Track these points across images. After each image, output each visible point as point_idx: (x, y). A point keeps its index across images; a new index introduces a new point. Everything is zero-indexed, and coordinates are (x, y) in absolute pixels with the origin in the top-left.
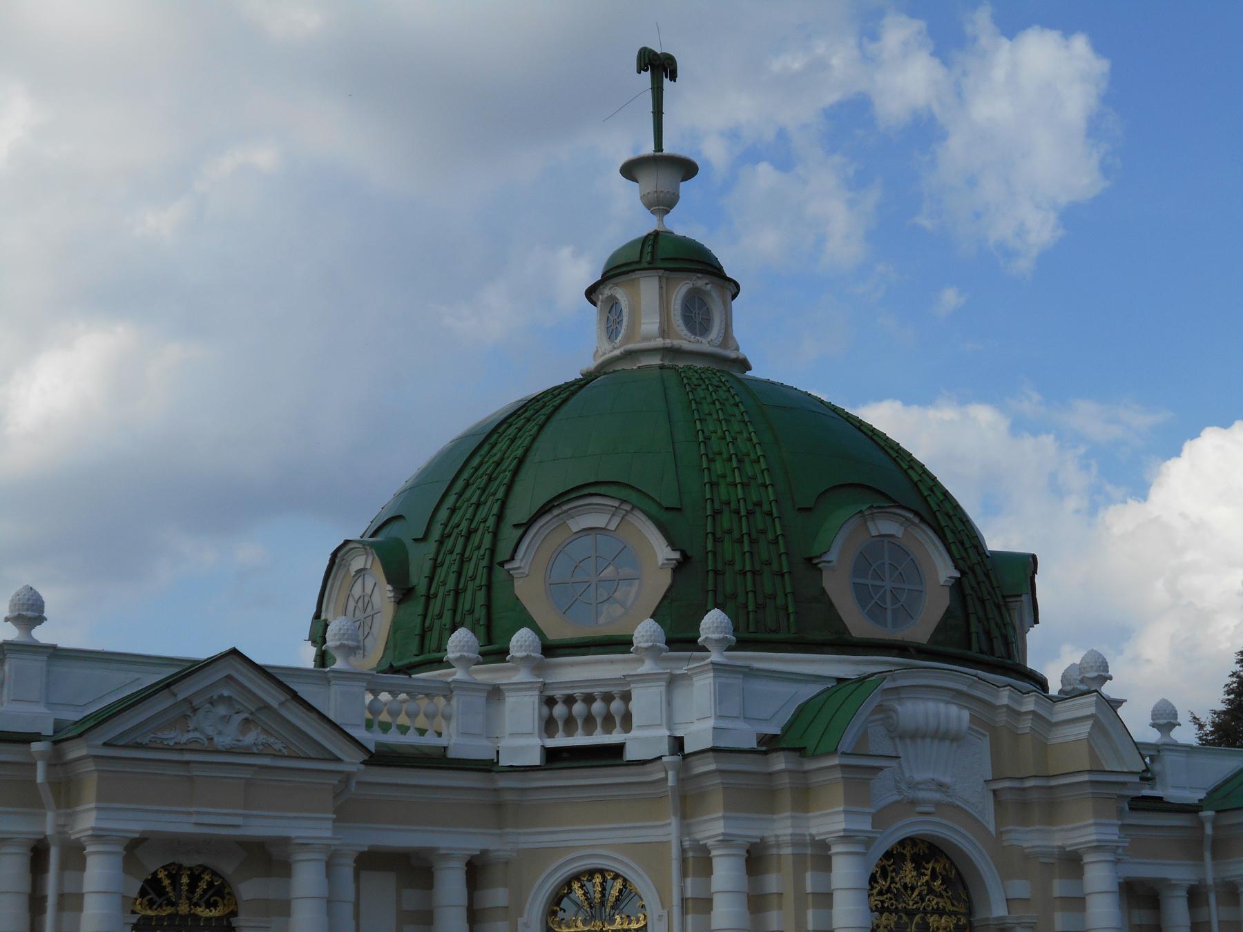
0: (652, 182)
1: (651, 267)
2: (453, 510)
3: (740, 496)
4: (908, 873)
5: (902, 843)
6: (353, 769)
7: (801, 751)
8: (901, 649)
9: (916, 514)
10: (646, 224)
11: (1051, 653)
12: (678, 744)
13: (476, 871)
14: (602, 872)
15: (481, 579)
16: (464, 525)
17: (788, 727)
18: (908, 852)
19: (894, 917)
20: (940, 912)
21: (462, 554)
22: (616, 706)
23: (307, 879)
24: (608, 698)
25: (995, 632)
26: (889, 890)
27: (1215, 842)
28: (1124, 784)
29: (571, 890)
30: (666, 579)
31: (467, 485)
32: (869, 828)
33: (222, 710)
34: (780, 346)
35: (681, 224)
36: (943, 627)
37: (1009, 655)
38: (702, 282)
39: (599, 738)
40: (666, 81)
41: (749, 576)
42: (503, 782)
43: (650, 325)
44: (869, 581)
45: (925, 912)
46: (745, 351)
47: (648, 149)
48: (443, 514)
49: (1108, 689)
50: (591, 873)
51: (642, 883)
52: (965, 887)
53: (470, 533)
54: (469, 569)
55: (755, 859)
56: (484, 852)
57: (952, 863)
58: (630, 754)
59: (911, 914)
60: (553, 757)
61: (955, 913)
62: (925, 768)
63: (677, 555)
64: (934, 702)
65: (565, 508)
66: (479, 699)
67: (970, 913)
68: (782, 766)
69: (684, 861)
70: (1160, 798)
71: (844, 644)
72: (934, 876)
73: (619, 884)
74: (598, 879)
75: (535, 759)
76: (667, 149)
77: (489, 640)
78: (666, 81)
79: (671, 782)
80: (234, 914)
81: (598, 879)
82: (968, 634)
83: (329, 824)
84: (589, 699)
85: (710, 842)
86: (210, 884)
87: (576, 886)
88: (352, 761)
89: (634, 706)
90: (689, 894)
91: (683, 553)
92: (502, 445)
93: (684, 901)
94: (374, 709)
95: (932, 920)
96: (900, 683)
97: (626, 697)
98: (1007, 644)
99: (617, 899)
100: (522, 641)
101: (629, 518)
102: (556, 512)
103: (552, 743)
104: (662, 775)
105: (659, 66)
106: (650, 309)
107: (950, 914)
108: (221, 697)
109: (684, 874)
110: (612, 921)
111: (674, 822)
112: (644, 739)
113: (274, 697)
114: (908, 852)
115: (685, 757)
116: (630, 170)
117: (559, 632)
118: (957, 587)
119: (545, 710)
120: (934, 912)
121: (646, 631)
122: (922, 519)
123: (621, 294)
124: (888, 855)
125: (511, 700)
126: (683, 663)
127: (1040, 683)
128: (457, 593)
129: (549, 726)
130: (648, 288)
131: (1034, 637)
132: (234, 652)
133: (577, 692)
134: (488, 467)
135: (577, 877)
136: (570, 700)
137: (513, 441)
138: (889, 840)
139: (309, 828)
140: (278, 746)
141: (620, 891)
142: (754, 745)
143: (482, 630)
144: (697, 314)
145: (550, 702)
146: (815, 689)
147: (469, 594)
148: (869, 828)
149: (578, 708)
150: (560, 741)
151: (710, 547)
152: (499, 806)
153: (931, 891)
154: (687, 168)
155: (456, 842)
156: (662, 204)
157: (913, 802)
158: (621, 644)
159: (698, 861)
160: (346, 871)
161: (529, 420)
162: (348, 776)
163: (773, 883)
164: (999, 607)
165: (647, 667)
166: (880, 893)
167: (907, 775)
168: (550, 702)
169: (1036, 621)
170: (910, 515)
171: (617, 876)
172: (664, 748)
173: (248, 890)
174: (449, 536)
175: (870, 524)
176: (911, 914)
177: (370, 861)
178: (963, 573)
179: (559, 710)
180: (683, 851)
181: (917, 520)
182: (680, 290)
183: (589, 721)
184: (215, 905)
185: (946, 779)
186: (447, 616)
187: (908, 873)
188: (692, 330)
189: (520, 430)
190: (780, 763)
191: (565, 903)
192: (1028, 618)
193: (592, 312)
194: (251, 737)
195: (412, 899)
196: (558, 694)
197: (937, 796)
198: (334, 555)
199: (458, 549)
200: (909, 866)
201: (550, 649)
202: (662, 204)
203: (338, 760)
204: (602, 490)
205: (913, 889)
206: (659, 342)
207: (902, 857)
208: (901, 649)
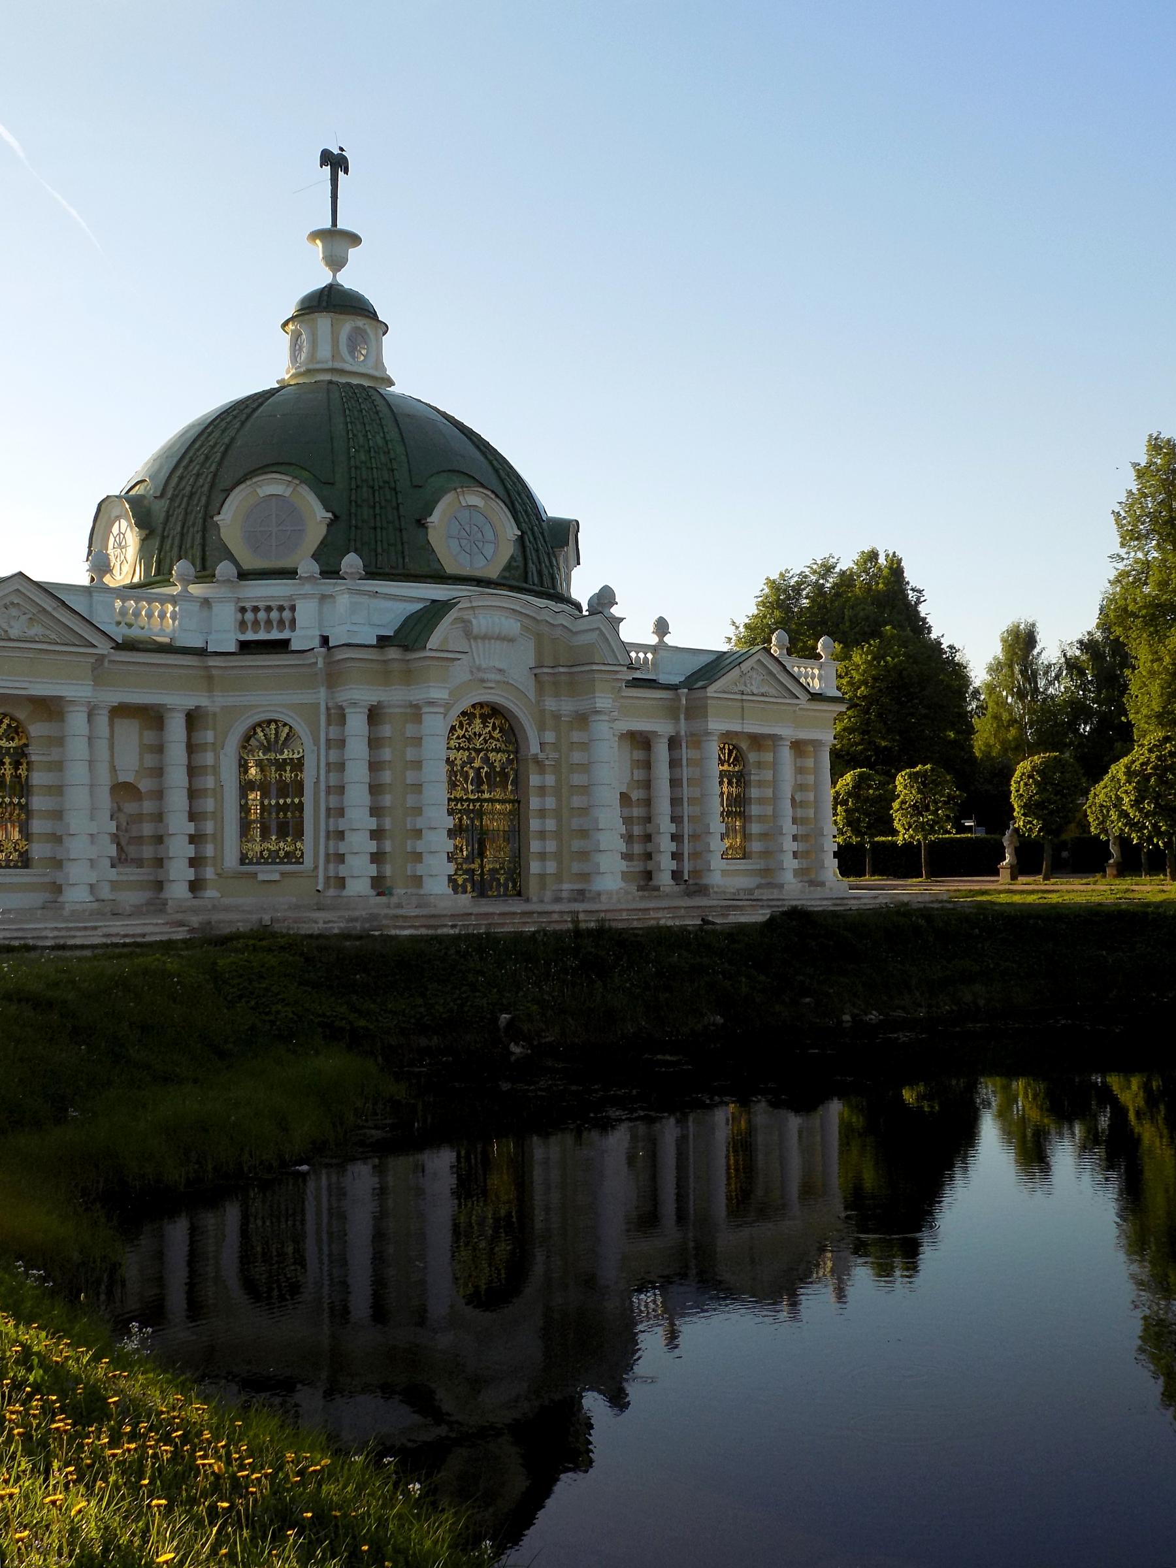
2: (181, 478)
3: (375, 476)
4: (477, 725)
5: (473, 706)
6: (105, 652)
7: (406, 648)
8: (479, 582)
9: (493, 492)
10: (321, 278)
11: (582, 586)
12: (325, 640)
13: (193, 719)
14: (276, 721)
15: (199, 527)
16: (188, 488)
17: (397, 632)
18: (477, 712)
19: (467, 753)
20: (498, 751)
21: (186, 510)
22: (286, 614)
23: (77, 722)
24: (281, 609)
25: (545, 572)
26: (464, 736)
27: (687, 709)
28: (617, 672)
29: (255, 733)
30: (323, 530)
31: (191, 461)
32: (446, 697)
33: (14, 612)
34: (420, 368)
35: (348, 279)
36: (508, 567)
37: (554, 587)
38: (361, 322)
39: (275, 635)
40: (341, 174)
41: (379, 530)
42: (212, 662)
43: (325, 352)
45: (487, 750)
48: (175, 480)
49: (615, 611)
50: (269, 722)
51: (301, 729)
52: (515, 735)
53: (192, 494)
54: (191, 518)
55: (374, 715)
56: (198, 707)
57: (506, 720)
58: (294, 646)
59: (478, 751)
60: (246, 647)
61: (508, 752)
62: (492, 657)
63: (330, 515)
64: (498, 613)
65: (254, 480)
66: (196, 607)
67: (516, 752)
68: (394, 656)
69: (329, 715)
70: (654, 680)
71: (441, 578)
72: (494, 728)
73: (286, 730)
74: (273, 726)
75: (232, 648)
77: (204, 568)
78: (341, 174)
79: (320, 664)
80: (26, 745)
81: (273, 726)
82: (526, 573)
83: (90, 688)
84: (269, 609)
85: (344, 704)
86: (9, 726)
87: (259, 730)
88: (104, 648)
90: (331, 736)
91: (334, 514)
92: (216, 434)
93: (328, 741)
94: (123, 612)
95: (491, 755)
96: (474, 604)
97: (293, 608)
98: (553, 578)
99: (286, 739)
100: (224, 569)
101: (299, 489)
102: (248, 483)
103: (243, 638)
104: (314, 660)
105: (335, 162)
107: (504, 752)
108: (12, 603)
109: (329, 723)
110: (282, 753)
111: (323, 690)
112: (303, 637)
113: (48, 604)
114: (477, 712)
115: (329, 649)
117: (250, 562)
118: (521, 540)
119: (239, 615)
120: (492, 750)
121: (308, 567)
122: (497, 496)
124: (464, 714)
125: (216, 608)
126: (329, 586)
127: (578, 606)
128: (182, 535)
129: (243, 625)
131: (576, 573)
132: (21, 573)
133: (261, 604)
134: (205, 450)
135: (259, 725)
136: (256, 609)
137: (223, 431)
138: (465, 704)
139: (76, 690)
140: (53, 636)
141: (288, 734)
142: (375, 642)
143: (198, 562)
145: (243, 610)
146: (420, 606)
147: (190, 535)
148: (446, 697)
149: (262, 615)
150: (250, 636)
151: (353, 510)
152: (210, 678)
153: (492, 737)
154: (355, 239)
155: (178, 700)
156: (336, 262)
157: (483, 681)
158: (290, 574)
159: (338, 716)
160: (103, 720)
161: (235, 417)
162: (101, 658)
163: (386, 730)
164: (548, 554)
165: (307, 588)
166: (458, 738)
167: (477, 662)
168: (243, 610)
169: (579, 564)
170: (489, 493)
171: (285, 725)
172: (316, 642)
173: (37, 729)
174: (177, 496)
175: (461, 498)
176: (478, 751)
177: (120, 711)
178: (523, 532)
179: (249, 616)
180: (328, 709)
181: (493, 496)
184: (13, 739)
185: (499, 665)
186: (176, 549)
187: (477, 725)
189: (228, 423)
190: (393, 653)
191: (253, 742)
192: (572, 560)
194: (36, 630)
195: (150, 737)
196: (248, 605)
197: (498, 677)
198: (100, 505)
199: (183, 506)
200: (478, 721)
201: (243, 575)
202: (336, 262)
203: (95, 646)
204: (280, 468)
205: (480, 735)
206: (329, 365)
207: (474, 715)
208: (479, 582)
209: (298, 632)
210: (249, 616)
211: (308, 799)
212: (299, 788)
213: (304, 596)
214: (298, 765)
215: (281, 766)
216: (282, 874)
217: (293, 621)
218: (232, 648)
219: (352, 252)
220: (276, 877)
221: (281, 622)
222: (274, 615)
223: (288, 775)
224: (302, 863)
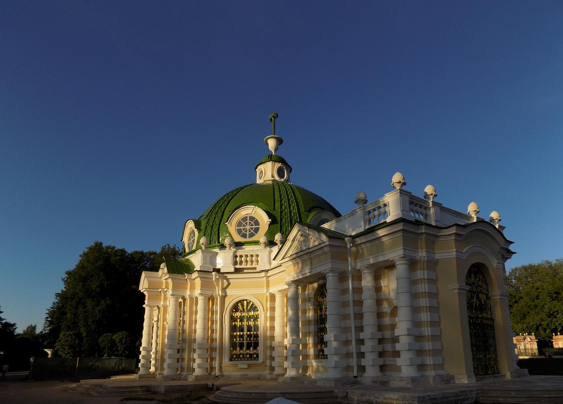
129: (235, 263)
150: (238, 266)
179: (238, 259)
214: (256, 318)
215: (249, 319)
223: (251, 323)
224: (258, 360)
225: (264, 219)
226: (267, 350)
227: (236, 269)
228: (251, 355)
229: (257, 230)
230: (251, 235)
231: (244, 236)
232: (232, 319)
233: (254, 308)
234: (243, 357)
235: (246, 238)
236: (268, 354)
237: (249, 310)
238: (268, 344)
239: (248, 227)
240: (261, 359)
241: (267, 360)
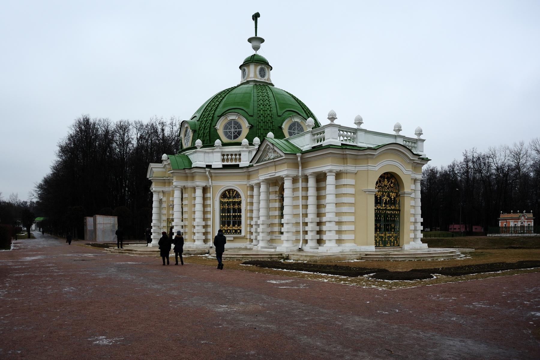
0: (256, 43)
1: (252, 62)
22: (238, 156)
24: (236, 155)
35: (261, 53)
39: (234, 163)
44: (233, 135)
46: (273, 82)
47: (254, 36)
50: (230, 189)
60: (225, 167)
75: (221, 167)
76: (258, 36)
89: (241, 157)
97: (240, 155)
100: (218, 142)
106: (253, 72)
116: (250, 40)
119: (222, 157)
123: (246, 68)
129: (223, 160)
130: (252, 67)
135: (227, 190)
136: (228, 155)
144: (262, 73)
149: (230, 157)
150: (226, 163)
154: (262, 41)
156: (256, 48)
158: (239, 144)
165: (244, 149)
168: (223, 155)
179: (226, 157)
182: (259, 68)
183: (232, 159)
188: (261, 76)
193: (240, 72)
201: (224, 145)
202: (256, 48)
206: (253, 79)
209: (242, 162)
210: (226, 157)
211: (243, 214)
212: (240, 211)
213: (244, 151)
214: (239, 203)
215: (234, 203)
216: (234, 238)
217: (240, 159)
218: (221, 167)
219: (262, 45)
220: (232, 239)
221: (236, 159)
222: (234, 157)
223: (236, 207)
225: (245, 126)
226: (247, 227)
227: (223, 165)
228: (236, 231)
229: (239, 133)
230: (236, 137)
231: (229, 137)
232: (222, 203)
233: (238, 195)
234: (230, 232)
235: (231, 139)
236: (248, 230)
237: (234, 197)
238: (248, 223)
239: (233, 130)
240: (243, 234)
241: (247, 234)
